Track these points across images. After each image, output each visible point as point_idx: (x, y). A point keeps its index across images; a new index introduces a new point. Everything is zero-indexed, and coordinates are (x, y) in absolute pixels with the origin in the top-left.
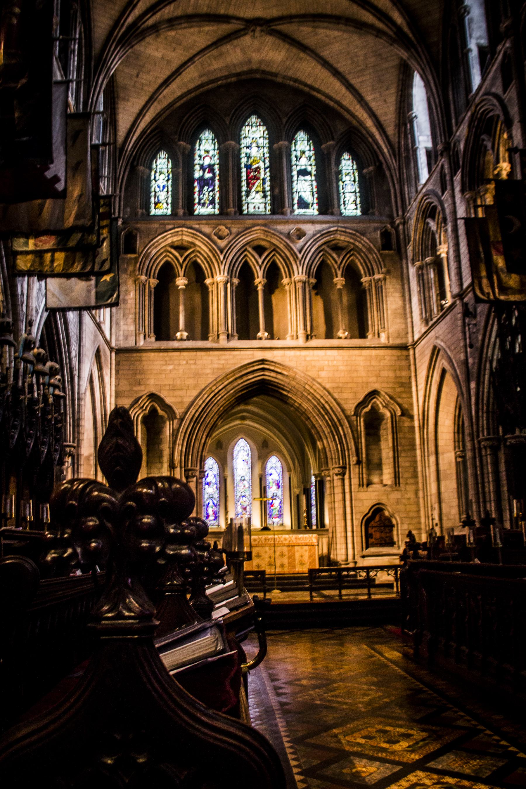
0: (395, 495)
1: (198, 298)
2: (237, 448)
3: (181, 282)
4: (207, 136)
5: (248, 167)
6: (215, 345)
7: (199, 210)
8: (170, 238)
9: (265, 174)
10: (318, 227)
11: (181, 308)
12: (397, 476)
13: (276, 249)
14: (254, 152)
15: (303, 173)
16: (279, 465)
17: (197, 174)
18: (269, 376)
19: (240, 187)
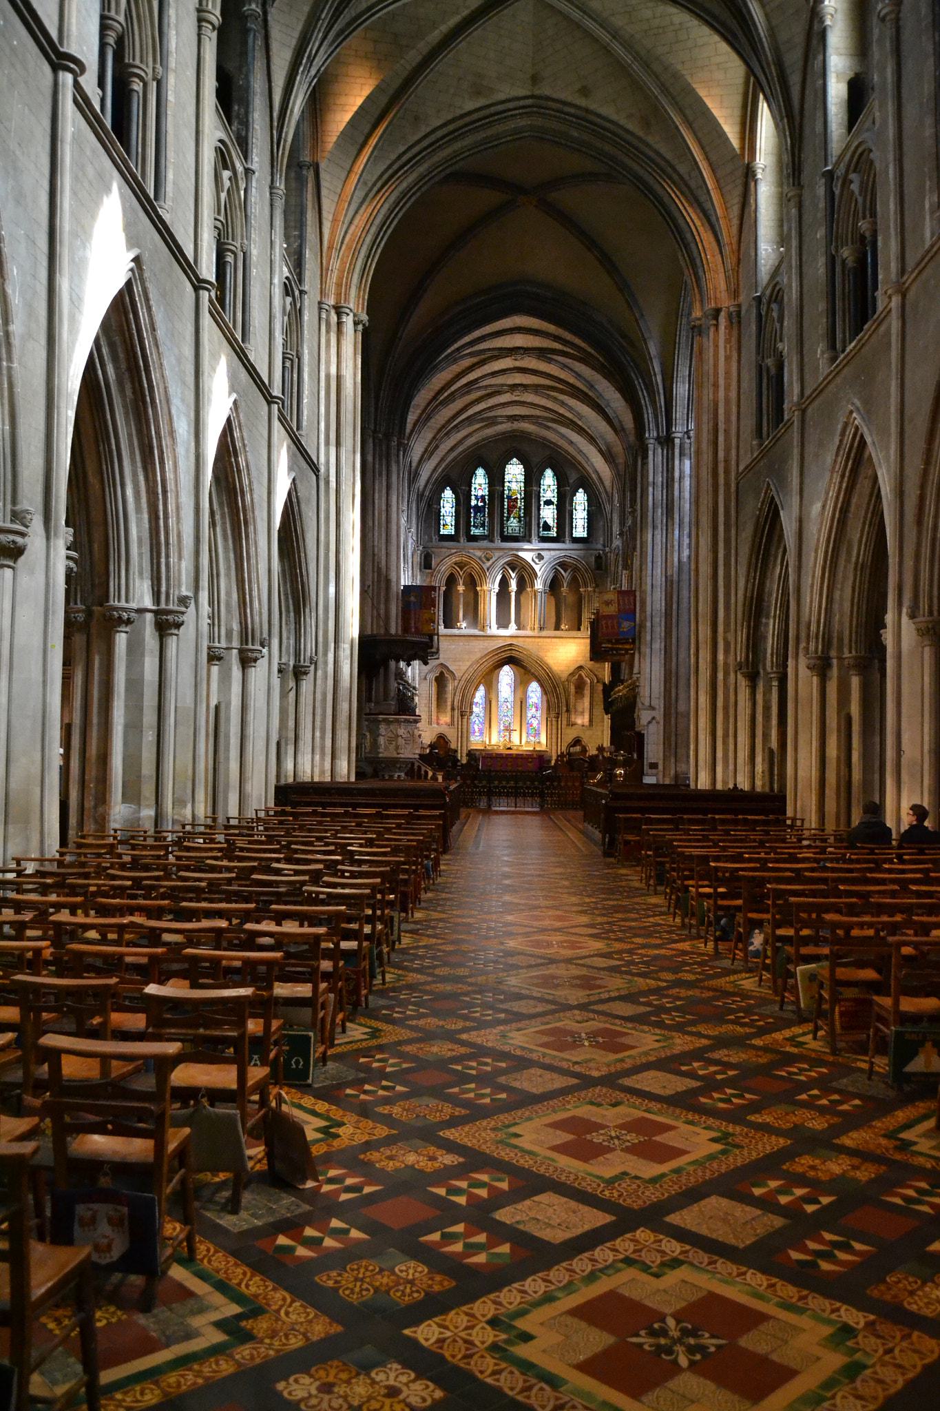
0: (588, 733)
1: (472, 595)
2: (502, 673)
3: (461, 588)
4: (480, 472)
5: (509, 498)
6: (481, 633)
7: (474, 531)
8: (454, 559)
9: (520, 504)
10: (553, 553)
11: (461, 606)
12: (591, 721)
13: (523, 567)
14: (514, 486)
15: (548, 503)
16: (539, 689)
17: (473, 503)
18: (514, 654)
19: (502, 513)
